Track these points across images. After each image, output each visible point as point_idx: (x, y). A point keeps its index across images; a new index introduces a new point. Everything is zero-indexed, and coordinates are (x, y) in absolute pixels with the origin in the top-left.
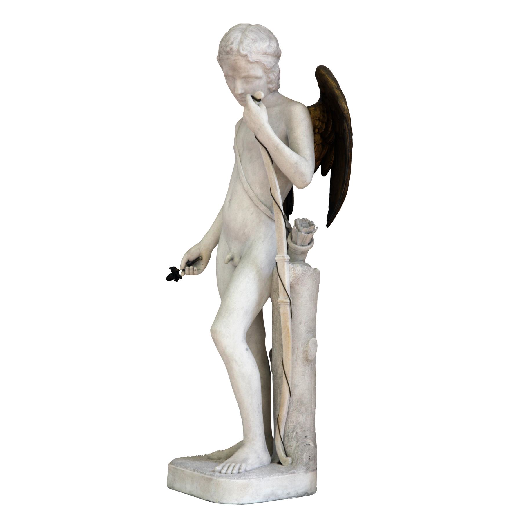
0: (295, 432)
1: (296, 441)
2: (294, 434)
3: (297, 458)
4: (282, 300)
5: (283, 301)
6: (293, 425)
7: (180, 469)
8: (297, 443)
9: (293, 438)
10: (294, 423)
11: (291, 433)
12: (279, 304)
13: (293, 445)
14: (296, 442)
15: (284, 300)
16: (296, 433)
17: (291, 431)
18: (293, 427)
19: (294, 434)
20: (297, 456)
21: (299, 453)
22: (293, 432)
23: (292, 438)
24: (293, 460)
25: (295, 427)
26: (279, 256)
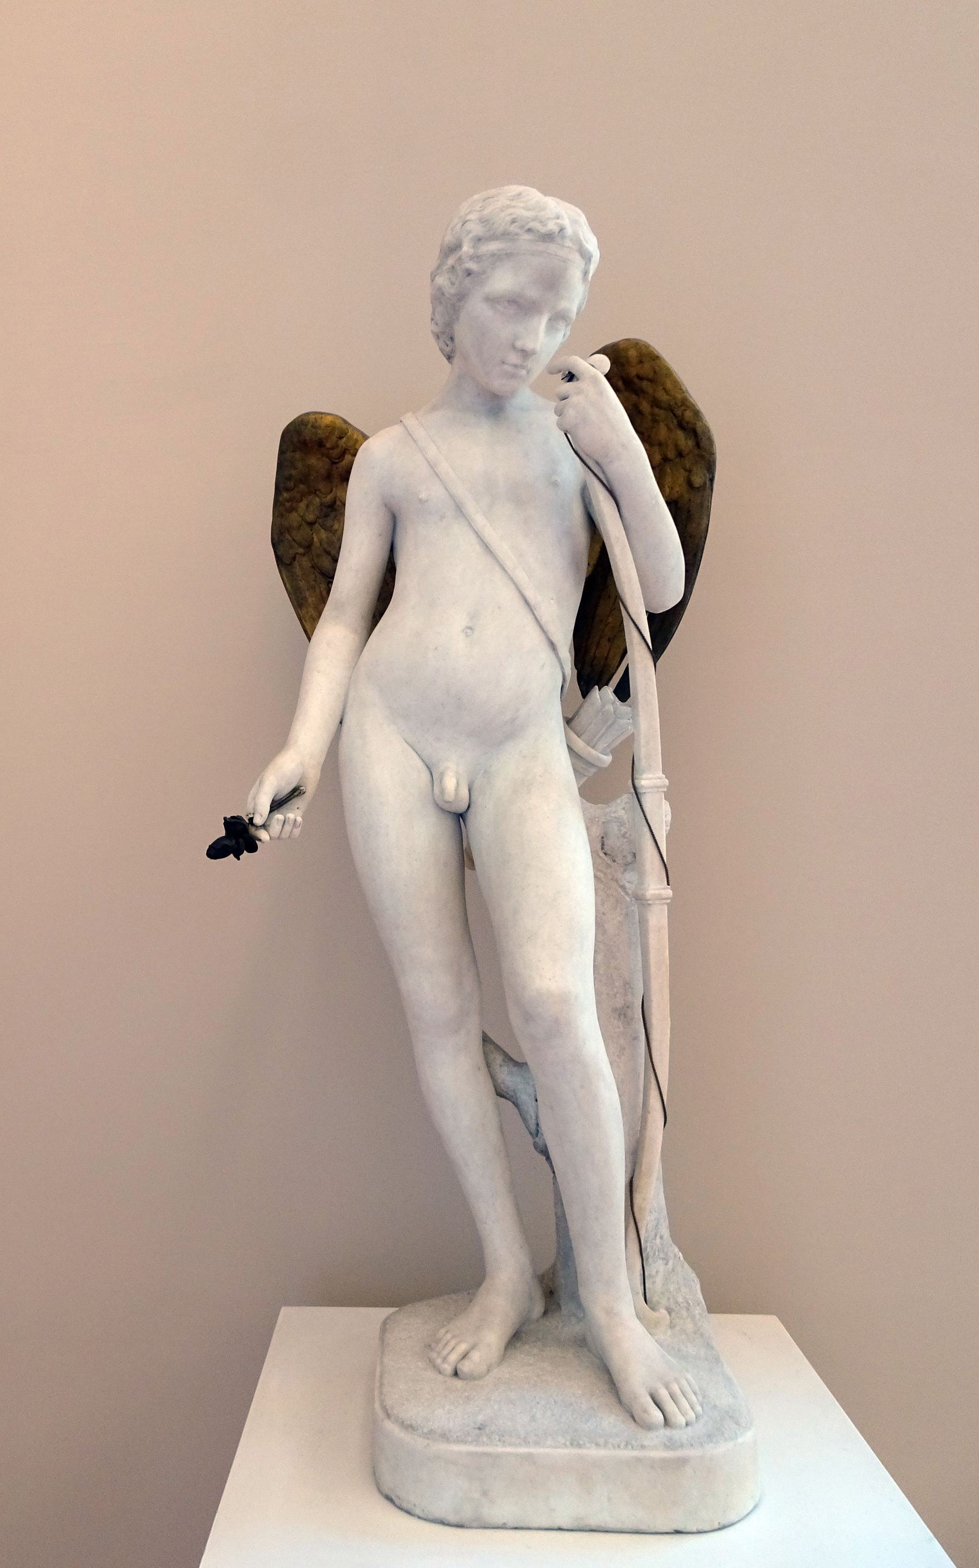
0: (658, 1237)
1: (663, 1259)
2: (658, 1241)
3: (686, 1305)
4: (657, 892)
5: (659, 895)
6: (655, 1219)
7: (510, 1454)
8: (666, 1264)
9: (657, 1253)
10: (655, 1211)
11: (652, 1240)
12: (650, 902)
13: (657, 1272)
14: (664, 1261)
15: (663, 892)
16: (661, 1237)
17: (653, 1233)
18: (655, 1223)
19: (658, 1241)
20: (680, 1299)
21: (683, 1289)
22: (656, 1235)
23: (655, 1253)
24: (669, 1311)
25: (658, 1220)
26: (650, 776)
